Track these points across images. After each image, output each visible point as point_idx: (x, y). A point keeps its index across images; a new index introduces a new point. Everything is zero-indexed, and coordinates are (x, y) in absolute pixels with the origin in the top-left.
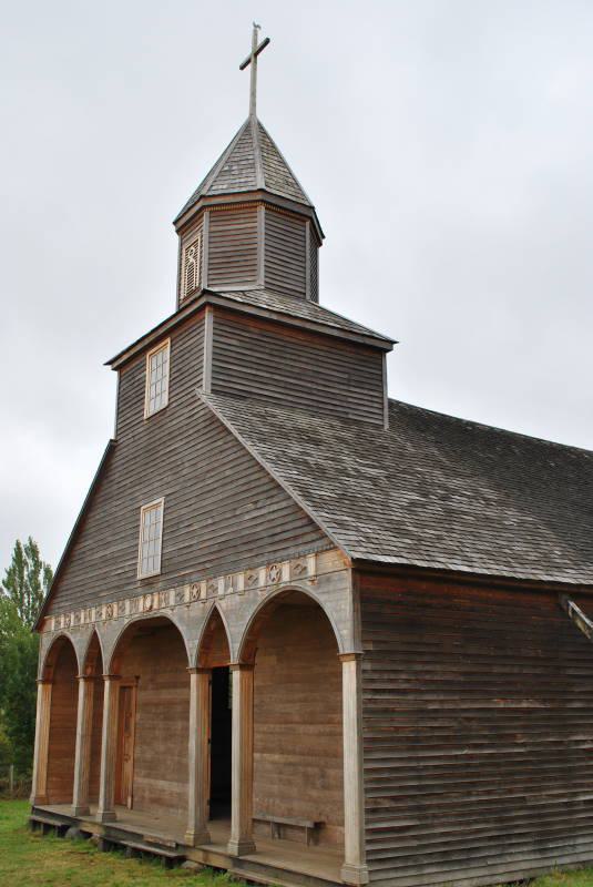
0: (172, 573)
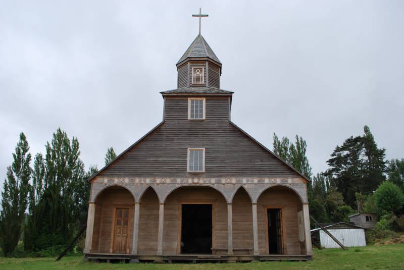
0: (209, 172)
